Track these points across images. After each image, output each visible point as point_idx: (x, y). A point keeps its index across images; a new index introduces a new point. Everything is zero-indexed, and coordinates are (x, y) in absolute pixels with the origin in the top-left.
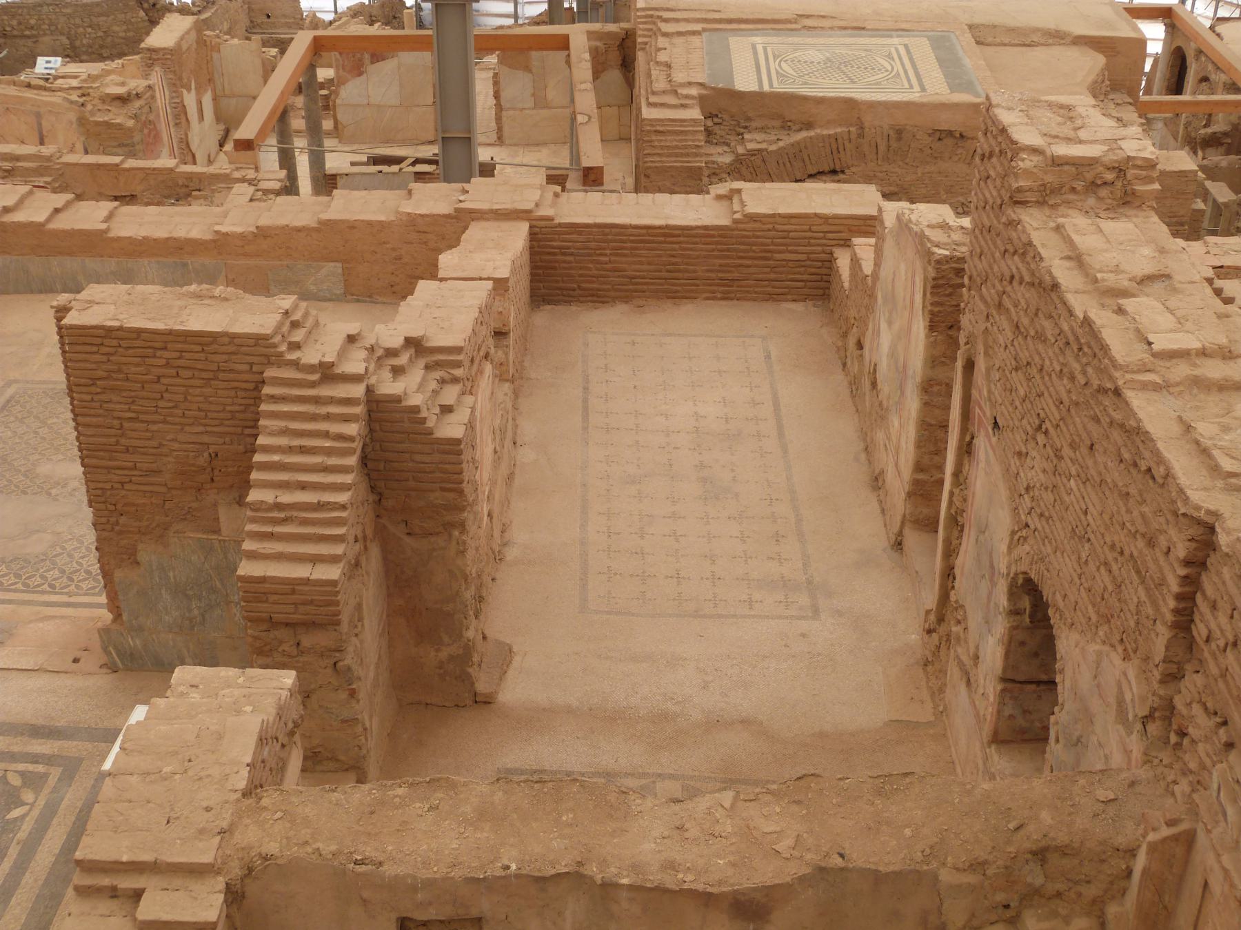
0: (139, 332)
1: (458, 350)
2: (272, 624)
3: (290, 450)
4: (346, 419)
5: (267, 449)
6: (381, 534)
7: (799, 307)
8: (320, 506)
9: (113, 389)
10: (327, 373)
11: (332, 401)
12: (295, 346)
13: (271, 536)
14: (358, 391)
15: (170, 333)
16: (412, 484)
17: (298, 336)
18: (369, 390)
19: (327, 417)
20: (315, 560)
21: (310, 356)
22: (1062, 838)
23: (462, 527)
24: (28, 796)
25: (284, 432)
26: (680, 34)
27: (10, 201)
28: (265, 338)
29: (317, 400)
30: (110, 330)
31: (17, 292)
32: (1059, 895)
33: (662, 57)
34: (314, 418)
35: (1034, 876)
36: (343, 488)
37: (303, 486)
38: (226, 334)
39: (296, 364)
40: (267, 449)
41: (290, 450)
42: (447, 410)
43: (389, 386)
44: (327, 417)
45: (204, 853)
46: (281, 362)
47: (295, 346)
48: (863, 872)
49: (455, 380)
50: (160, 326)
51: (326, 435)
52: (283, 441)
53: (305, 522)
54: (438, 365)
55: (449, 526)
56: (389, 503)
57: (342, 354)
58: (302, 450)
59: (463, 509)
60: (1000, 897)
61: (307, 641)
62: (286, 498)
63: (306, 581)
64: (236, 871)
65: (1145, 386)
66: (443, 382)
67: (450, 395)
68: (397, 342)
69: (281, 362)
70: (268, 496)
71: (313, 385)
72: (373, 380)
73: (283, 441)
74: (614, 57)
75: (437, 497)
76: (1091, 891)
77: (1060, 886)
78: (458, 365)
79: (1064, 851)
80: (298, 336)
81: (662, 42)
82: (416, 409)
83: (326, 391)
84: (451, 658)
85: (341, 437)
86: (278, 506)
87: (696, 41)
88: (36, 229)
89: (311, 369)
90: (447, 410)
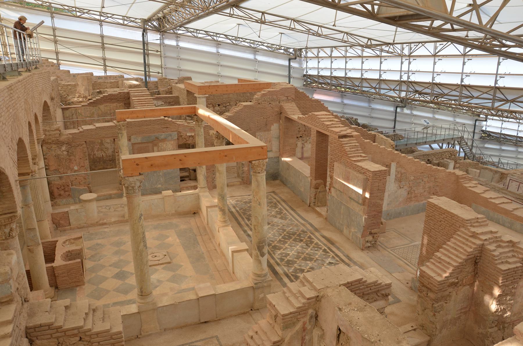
0: (440, 208)
2: (424, 286)
3: (453, 248)
9: (432, 220)
11: (471, 242)
15: (446, 210)
16: (487, 276)
19: (467, 245)
29: (467, 240)
30: (435, 205)
34: (464, 243)
37: (449, 257)
38: (457, 216)
41: (453, 248)
50: (445, 208)
51: (463, 248)
52: (452, 245)
53: (444, 265)
58: (455, 249)
61: (430, 294)
63: (432, 278)
84: (482, 333)
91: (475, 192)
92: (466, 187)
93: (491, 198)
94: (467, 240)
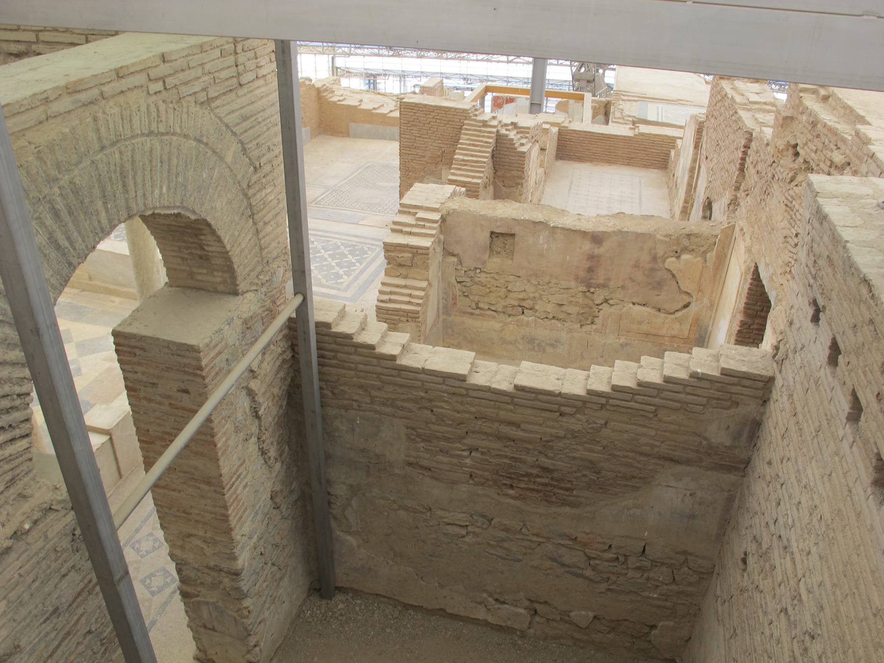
1: (529, 128)
3: (470, 145)
4: (489, 137)
5: (462, 144)
6: (495, 184)
7: (656, 171)
8: (477, 162)
10: (485, 124)
11: (485, 132)
12: (476, 116)
13: (460, 169)
14: (495, 130)
15: (436, 106)
17: (477, 113)
18: (498, 131)
20: (473, 177)
21: (479, 118)
22: (696, 232)
23: (522, 184)
24: (370, 253)
25: (468, 140)
26: (629, 100)
27: (376, 106)
28: (467, 110)
29: (480, 131)
31: (373, 138)
32: (693, 250)
33: (620, 107)
34: (479, 136)
35: (685, 242)
36: (485, 157)
37: (472, 156)
39: (475, 120)
40: (462, 144)
41: (470, 145)
42: (522, 145)
43: (503, 131)
44: (483, 136)
45: (437, 206)
46: (470, 119)
47: (476, 116)
48: (633, 233)
49: (526, 138)
51: (482, 141)
52: (468, 142)
53: (471, 166)
54: (521, 132)
55: (517, 184)
56: (499, 174)
57: (490, 120)
58: (474, 145)
59: (523, 179)
60: (675, 248)
62: (466, 158)
64: (444, 212)
65: (744, 109)
66: (522, 138)
67: (524, 141)
68: (509, 122)
69: (470, 119)
70: (461, 157)
71: (480, 127)
72: (499, 128)
73: (468, 142)
74: (602, 111)
75: (515, 173)
76: (702, 249)
77: (694, 247)
78: (528, 133)
79: (697, 236)
80: (477, 113)
81: (621, 102)
82: (512, 140)
83: (483, 129)
85: (486, 142)
86: (463, 160)
87: (635, 103)
88: (384, 115)
89: (480, 121)
90: (522, 145)
91: (349, 106)
92: (334, 103)
93: (374, 109)
94: (480, 131)
